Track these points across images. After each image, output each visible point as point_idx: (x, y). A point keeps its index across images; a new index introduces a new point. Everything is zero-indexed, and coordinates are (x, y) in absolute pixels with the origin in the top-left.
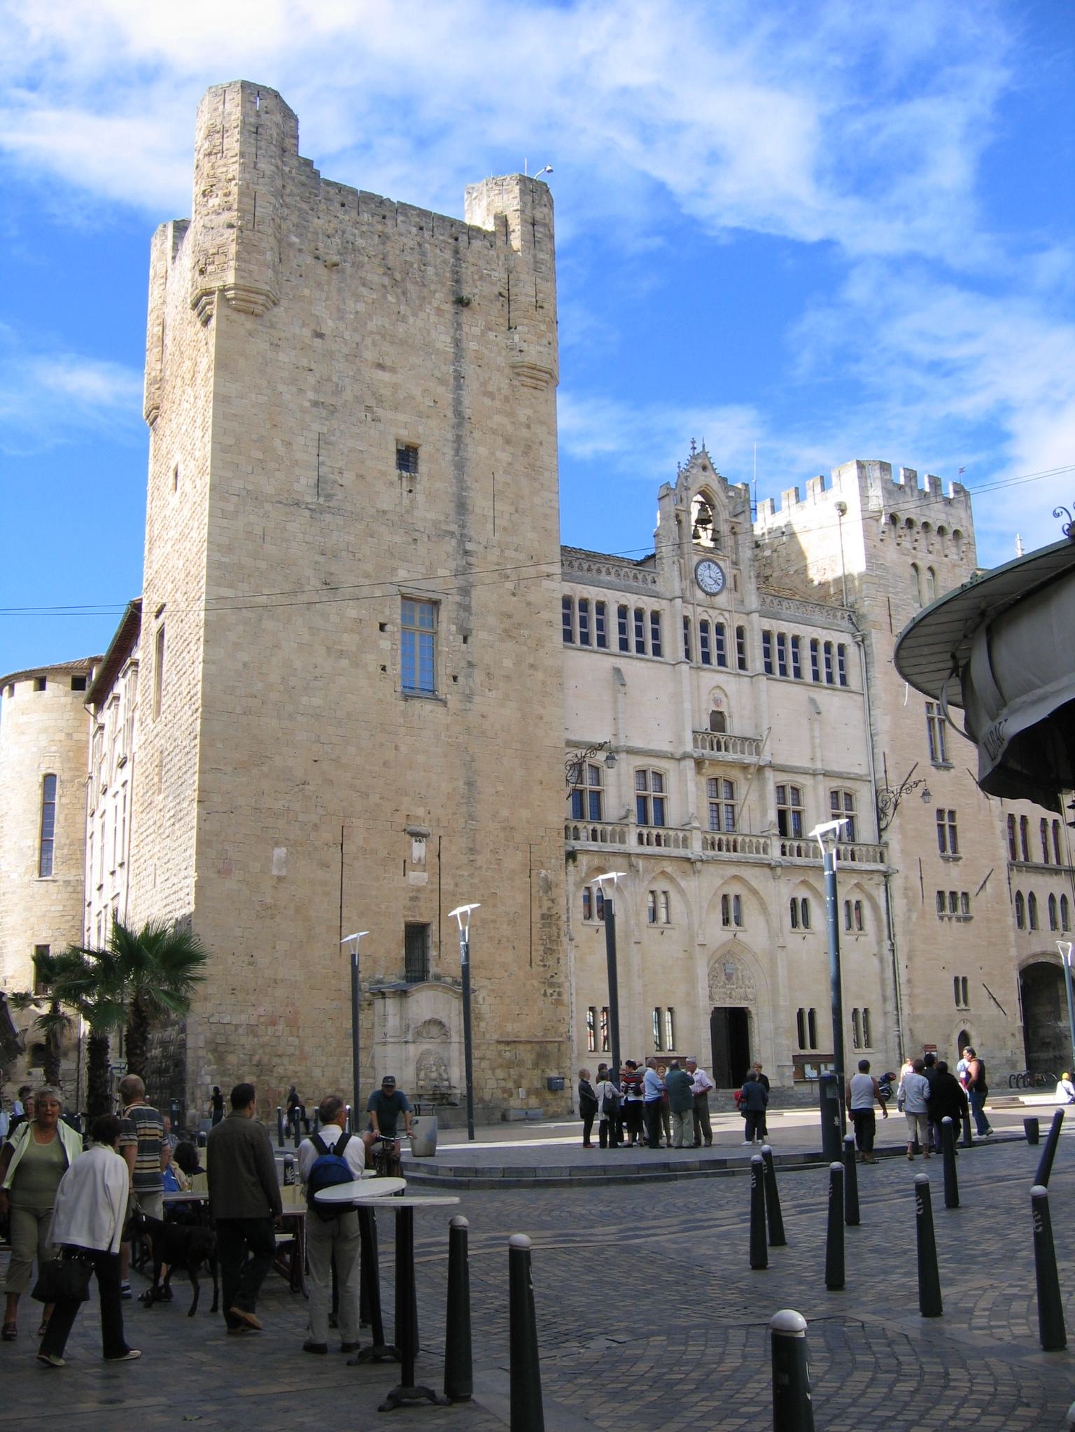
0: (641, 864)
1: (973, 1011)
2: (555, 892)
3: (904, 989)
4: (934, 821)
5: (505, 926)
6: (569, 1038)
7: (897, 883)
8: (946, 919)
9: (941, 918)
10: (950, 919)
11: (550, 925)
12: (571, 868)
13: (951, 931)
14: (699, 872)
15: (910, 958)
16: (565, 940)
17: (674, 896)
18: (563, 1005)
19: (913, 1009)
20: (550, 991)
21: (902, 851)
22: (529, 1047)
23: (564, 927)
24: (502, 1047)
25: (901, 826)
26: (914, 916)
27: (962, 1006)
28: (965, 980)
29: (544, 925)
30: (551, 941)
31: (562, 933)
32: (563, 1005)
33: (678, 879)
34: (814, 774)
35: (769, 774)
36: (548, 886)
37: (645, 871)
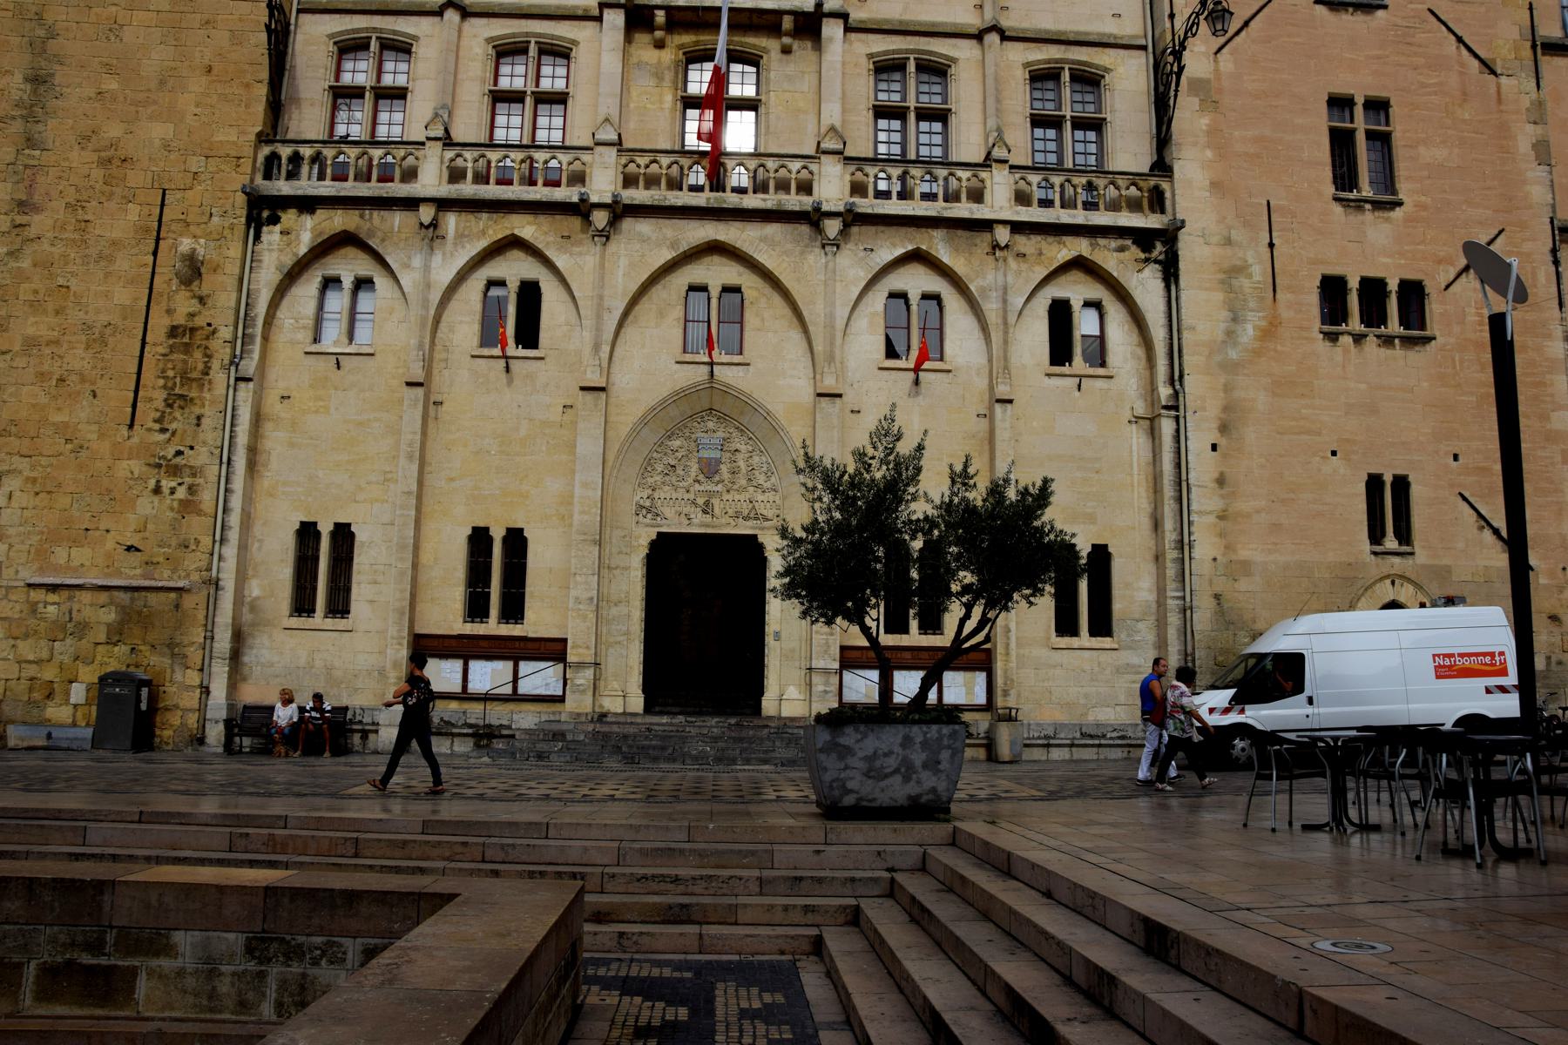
0: (451, 221)
1: (1422, 556)
2: (207, 285)
3: (1203, 501)
4: (1319, 123)
5: (80, 352)
6: (216, 584)
7: (1190, 249)
8: (1346, 340)
9: (1333, 337)
10: (1358, 339)
11: (187, 349)
12: (271, 235)
13: (1368, 364)
14: (605, 235)
15: (1224, 428)
16: (219, 378)
17: (551, 296)
18: (200, 513)
19: (1228, 548)
20: (167, 484)
21: (1215, 185)
22: (103, 597)
23: (222, 353)
24: (37, 595)
25: (1212, 132)
26: (1248, 332)
27: (1391, 543)
28: (1401, 484)
29: (172, 349)
30: (186, 379)
31: (215, 365)
32: (200, 513)
33: (549, 253)
34: (979, 37)
35: (832, 30)
36: (193, 271)
37: (461, 236)
